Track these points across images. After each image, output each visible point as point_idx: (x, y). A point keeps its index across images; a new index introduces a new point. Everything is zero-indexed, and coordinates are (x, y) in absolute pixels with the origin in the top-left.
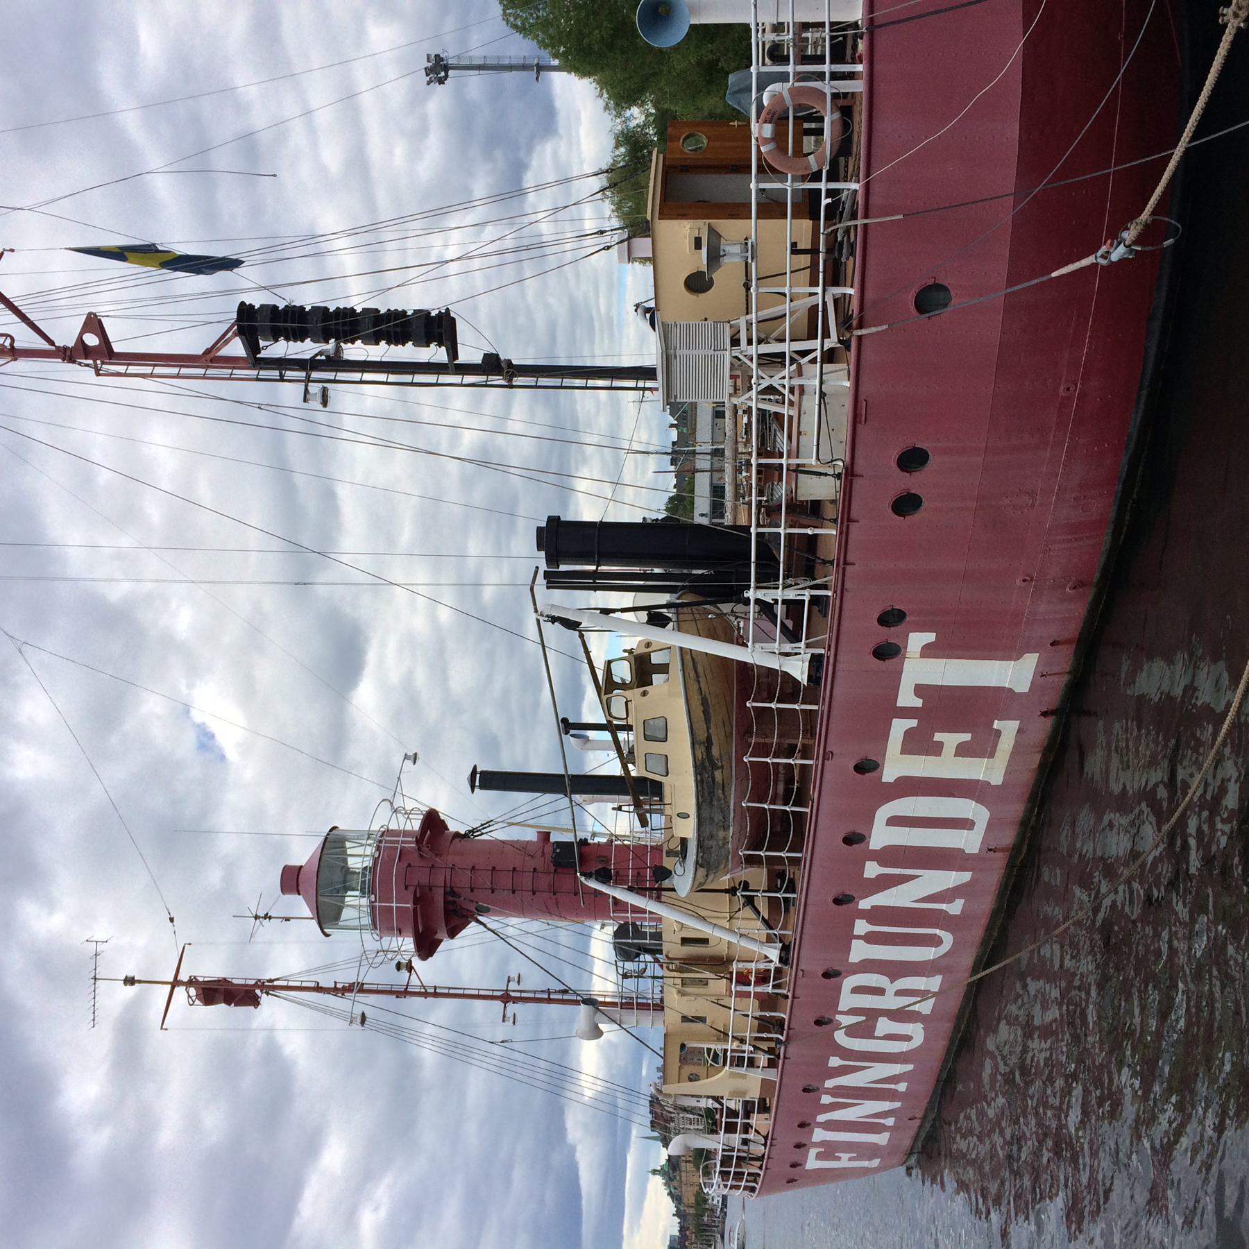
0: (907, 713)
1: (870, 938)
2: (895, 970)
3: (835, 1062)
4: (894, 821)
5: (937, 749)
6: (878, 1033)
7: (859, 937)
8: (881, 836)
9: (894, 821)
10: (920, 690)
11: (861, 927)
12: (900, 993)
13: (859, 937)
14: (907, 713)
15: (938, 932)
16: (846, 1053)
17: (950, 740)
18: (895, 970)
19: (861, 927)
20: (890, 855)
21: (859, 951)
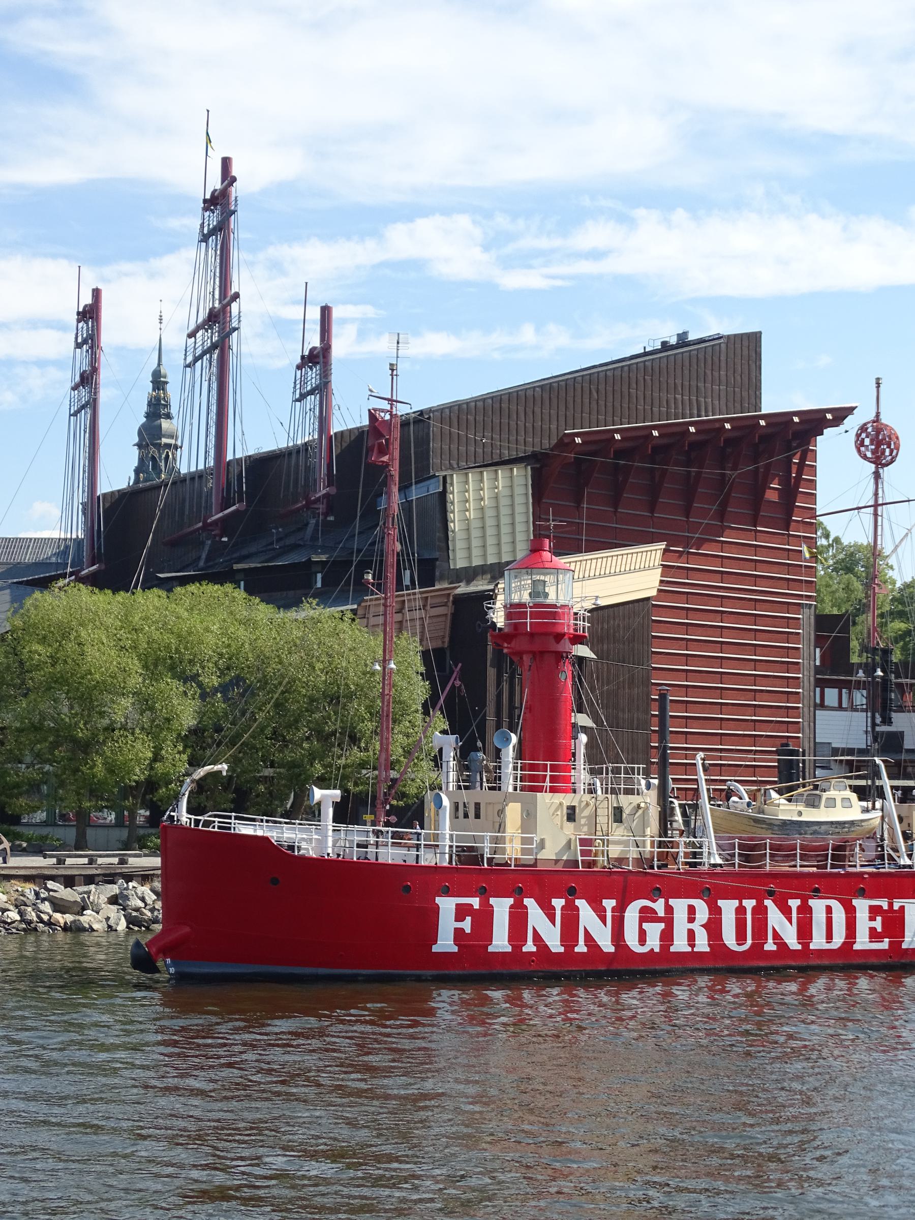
0: (891, 905)
1: (741, 910)
2: (714, 927)
3: (609, 904)
4: (829, 909)
5: (872, 919)
6: (645, 926)
7: (741, 903)
8: (818, 906)
9: (829, 909)
10: (902, 908)
11: (749, 904)
12: (691, 935)
13: (741, 903)
14: (891, 905)
15: (749, 942)
16: (620, 910)
17: (878, 924)
18: (714, 927)
19: (749, 904)
20: (805, 910)
21: (728, 907)
